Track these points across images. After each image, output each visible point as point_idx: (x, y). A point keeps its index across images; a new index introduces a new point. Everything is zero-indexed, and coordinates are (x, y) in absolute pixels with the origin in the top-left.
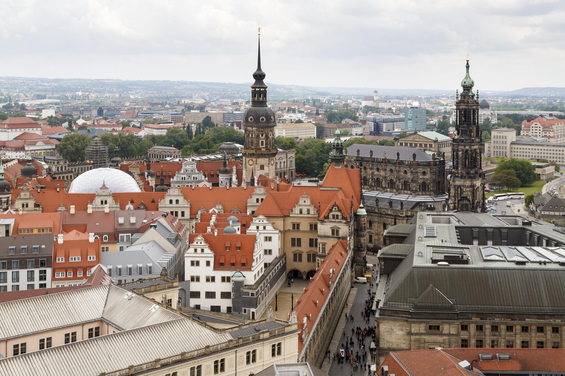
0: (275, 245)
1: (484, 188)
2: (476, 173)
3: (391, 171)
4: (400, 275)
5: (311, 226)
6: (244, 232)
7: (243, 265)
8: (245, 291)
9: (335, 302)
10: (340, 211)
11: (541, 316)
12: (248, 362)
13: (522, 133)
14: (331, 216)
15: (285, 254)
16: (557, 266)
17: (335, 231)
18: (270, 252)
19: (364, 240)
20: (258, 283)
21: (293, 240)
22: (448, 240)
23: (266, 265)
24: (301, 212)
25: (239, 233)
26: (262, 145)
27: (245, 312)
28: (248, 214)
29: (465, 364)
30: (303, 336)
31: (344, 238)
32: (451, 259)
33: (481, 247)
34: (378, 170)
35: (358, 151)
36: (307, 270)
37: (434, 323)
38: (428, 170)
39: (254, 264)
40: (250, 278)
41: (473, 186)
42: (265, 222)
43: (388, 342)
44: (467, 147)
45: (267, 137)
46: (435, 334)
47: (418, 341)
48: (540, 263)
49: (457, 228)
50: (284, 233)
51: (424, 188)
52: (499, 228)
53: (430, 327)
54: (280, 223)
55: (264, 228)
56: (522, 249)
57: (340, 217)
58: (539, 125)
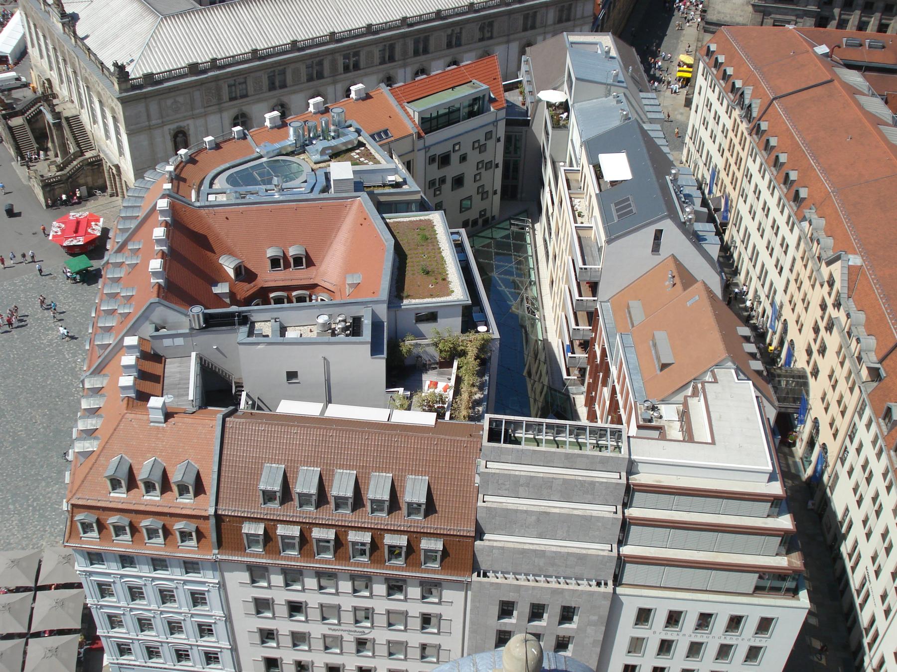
29: (823, 49)
43: (719, 12)
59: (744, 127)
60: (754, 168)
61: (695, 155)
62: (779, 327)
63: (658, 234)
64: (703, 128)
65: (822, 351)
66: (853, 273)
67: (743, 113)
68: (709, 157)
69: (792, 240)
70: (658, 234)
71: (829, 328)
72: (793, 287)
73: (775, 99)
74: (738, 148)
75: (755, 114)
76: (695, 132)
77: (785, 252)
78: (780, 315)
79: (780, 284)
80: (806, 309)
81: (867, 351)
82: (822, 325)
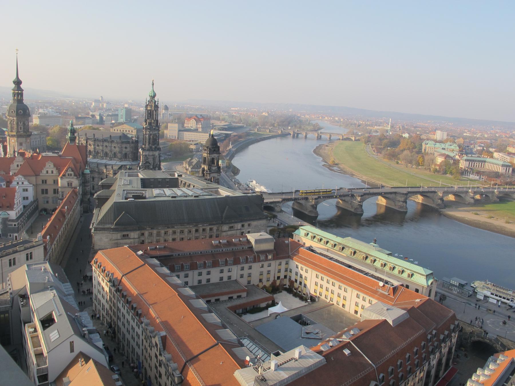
0: (31, 194)
1: (160, 156)
2: (156, 148)
3: (106, 146)
4: (107, 207)
5: (54, 181)
6: (8, 186)
7: (8, 207)
8: (9, 223)
9: (69, 226)
10: (72, 171)
11: (182, 224)
12: (10, 265)
13: (185, 125)
14: (67, 175)
15: (37, 199)
16: (193, 198)
17: (70, 184)
18: (27, 198)
19: (88, 189)
20: (18, 218)
21: (43, 190)
22: (136, 186)
23: (24, 207)
24: (47, 172)
25: (5, 187)
26: (21, 129)
27: (10, 236)
28: (11, 174)
29: (140, 252)
30: (47, 247)
31: (75, 188)
32: (135, 197)
33: (153, 189)
34: (98, 146)
35: (86, 134)
36: (52, 209)
37: (125, 233)
38: (128, 146)
39: (15, 206)
40: (13, 214)
41: (153, 155)
42: (23, 179)
44: (151, 133)
45: (24, 124)
46: (126, 239)
47: (117, 243)
48: (184, 196)
49: (141, 179)
50: (36, 186)
51: (125, 157)
52: (165, 179)
53: (124, 236)
54: (33, 179)
55: (23, 183)
56: (175, 189)
57: (73, 175)
58: (194, 121)
59: (113, 289)
60: (120, 306)
61: (98, 306)
62: (143, 371)
63: (72, 343)
64: (99, 294)
65: (160, 376)
66: (164, 339)
67: (112, 284)
68: (103, 306)
69: (140, 332)
70: (72, 343)
71: (160, 365)
72: (144, 351)
73: (123, 276)
74: (113, 299)
75: (116, 284)
76: (96, 296)
77: (139, 338)
78: (143, 366)
79: (140, 353)
80: (151, 360)
81: (174, 370)
82: (158, 365)
